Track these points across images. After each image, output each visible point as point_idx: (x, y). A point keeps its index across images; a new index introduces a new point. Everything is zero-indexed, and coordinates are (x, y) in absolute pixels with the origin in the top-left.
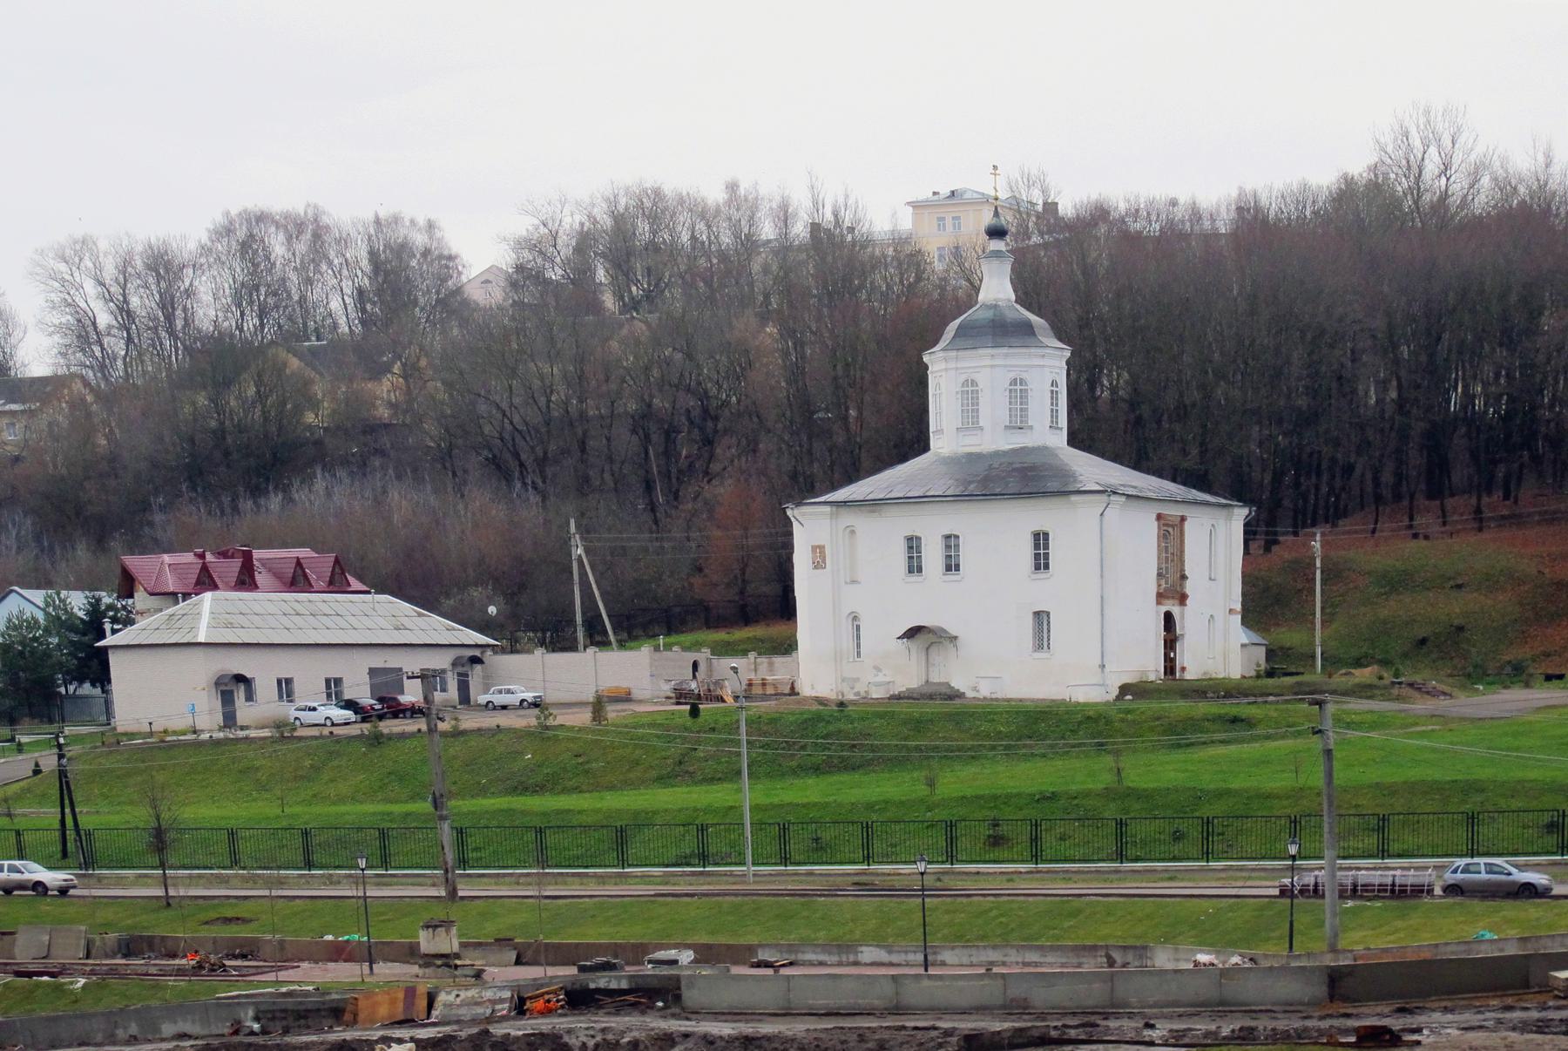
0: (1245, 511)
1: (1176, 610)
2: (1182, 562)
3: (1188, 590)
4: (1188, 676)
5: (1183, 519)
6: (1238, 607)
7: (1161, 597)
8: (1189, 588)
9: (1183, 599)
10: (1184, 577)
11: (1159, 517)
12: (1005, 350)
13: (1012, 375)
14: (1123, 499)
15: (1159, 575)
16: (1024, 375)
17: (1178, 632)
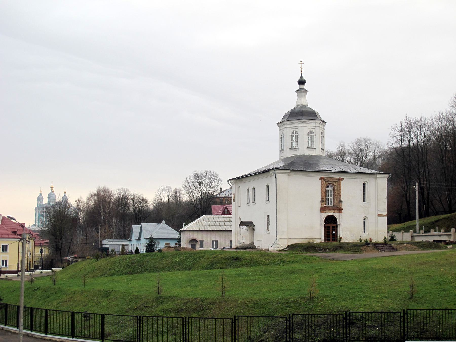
0: (387, 176)
1: (336, 215)
2: (340, 196)
3: (343, 207)
4: (344, 241)
5: (340, 179)
6: (385, 213)
7: (323, 209)
8: (343, 206)
9: (340, 210)
10: (341, 202)
11: (321, 179)
12: (289, 122)
13: (292, 130)
14: (289, 171)
15: (322, 201)
16: (297, 130)
17: (338, 223)
